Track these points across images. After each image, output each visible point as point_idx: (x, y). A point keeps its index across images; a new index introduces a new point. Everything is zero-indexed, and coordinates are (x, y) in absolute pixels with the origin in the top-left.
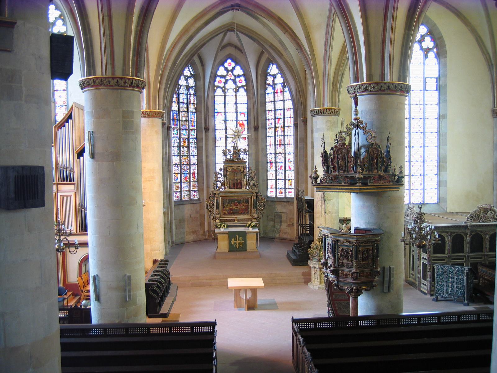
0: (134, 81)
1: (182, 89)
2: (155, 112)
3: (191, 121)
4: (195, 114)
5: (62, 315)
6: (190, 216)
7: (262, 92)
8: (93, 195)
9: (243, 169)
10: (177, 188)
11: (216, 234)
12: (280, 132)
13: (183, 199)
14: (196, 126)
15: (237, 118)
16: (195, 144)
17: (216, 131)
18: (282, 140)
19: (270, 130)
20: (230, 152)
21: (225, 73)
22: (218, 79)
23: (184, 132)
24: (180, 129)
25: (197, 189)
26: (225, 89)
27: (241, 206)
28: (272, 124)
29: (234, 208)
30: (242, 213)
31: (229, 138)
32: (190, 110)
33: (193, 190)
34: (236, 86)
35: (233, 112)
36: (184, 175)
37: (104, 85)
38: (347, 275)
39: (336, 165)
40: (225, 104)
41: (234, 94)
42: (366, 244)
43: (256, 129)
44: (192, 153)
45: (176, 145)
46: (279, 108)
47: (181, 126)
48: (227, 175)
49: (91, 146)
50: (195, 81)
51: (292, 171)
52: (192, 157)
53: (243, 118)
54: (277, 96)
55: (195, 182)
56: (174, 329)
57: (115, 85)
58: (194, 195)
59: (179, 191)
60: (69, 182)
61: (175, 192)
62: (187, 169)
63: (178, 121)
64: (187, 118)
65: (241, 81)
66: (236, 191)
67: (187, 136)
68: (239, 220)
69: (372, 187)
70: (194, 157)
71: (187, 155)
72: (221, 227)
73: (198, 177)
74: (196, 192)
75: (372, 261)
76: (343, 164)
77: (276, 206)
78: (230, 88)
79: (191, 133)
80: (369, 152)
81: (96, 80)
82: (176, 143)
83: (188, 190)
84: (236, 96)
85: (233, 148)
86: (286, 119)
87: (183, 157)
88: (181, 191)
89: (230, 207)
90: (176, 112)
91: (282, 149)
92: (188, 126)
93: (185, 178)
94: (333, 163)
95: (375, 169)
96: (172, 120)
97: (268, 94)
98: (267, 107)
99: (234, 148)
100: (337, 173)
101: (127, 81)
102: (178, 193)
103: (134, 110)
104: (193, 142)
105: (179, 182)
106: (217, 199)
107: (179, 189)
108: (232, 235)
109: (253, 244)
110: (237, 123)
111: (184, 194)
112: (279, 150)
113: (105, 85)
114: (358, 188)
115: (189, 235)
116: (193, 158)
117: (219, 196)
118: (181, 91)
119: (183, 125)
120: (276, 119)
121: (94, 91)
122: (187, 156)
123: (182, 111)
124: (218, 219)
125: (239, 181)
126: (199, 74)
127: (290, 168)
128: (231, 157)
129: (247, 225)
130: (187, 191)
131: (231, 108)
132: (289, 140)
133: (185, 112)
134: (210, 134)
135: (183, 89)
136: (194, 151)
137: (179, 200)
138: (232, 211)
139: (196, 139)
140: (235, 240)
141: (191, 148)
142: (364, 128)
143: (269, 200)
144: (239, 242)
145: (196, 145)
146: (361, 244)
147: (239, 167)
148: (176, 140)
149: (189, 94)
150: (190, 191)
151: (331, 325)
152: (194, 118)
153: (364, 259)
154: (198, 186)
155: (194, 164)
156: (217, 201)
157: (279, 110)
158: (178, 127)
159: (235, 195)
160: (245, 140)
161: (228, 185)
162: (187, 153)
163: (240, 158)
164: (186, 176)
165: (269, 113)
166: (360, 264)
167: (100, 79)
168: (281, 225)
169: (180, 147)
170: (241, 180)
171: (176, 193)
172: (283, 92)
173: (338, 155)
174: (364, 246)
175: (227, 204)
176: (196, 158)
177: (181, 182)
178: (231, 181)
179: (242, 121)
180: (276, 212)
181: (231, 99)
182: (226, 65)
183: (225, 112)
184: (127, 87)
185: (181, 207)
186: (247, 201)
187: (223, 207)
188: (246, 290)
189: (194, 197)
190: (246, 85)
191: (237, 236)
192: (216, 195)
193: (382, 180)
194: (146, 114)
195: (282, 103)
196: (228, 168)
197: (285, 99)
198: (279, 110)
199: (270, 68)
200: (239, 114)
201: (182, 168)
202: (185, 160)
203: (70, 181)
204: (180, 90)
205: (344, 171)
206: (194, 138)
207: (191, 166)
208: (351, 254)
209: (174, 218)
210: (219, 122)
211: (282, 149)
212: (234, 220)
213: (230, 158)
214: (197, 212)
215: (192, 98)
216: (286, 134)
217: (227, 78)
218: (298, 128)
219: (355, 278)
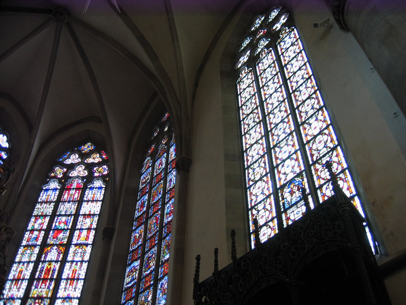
12: (53, 255)
18: (54, 270)
28: (37, 239)
54: (66, 194)
86: (77, 233)
91: (49, 288)
98: (36, 210)
112: (40, 290)
120: (51, 232)
132: (74, 272)
172: (83, 190)
198: (65, 215)
211: (49, 288)
216: (70, 258)
218: (111, 239)
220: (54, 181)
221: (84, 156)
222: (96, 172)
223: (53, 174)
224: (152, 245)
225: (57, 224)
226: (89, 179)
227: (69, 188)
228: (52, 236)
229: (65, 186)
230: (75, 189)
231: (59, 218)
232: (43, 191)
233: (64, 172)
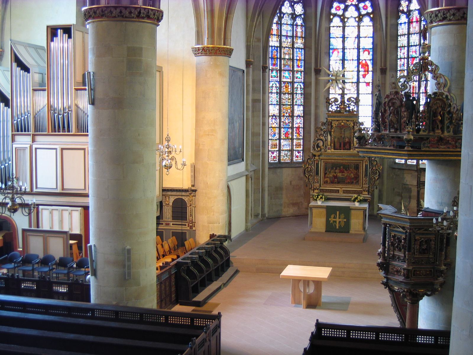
0: (142, 11)
1: (285, 18)
2: (219, 48)
3: (297, 60)
4: (303, 51)
5: (64, 289)
6: (291, 184)
7: (393, 21)
8: (92, 149)
9: (353, 125)
10: (275, 146)
11: (311, 208)
13: (282, 161)
16: (302, 89)
18: (416, 87)
19: (401, 73)
20: (337, 102)
23: (286, 74)
24: (280, 70)
25: (302, 149)
26: (345, 17)
27: (348, 173)
29: (340, 175)
30: (349, 183)
31: (347, 83)
32: (296, 46)
33: (296, 149)
34: (360, 14)
36: (284, 130)
37: (106, 16)
38: (398, 272)
39: (387, 121)
40: (344, 37)
41: (356, 24)
42: (424, 232)
43: (383, 71)
44: (296, 102)
45: (274, 90)
46: (414, 43)
48: (331, 132)
49: (91, 89)
50: (304, 7)
52: (296, 107)
53: (366, 57)
54: (412, 27)
55: (300, 139)
56: (170, 318)
57: (118, 16)
58: (297, 157)
59: (277, 151)
60: (20, 133)
61: (271, 151)
62: (289, 123)
63: (279, 60)
64: (291, 56)
66: (341, 153)
67: (291, 79)
68: (345, 192)
69: (427, 153)
71: (289, 103)
72: (318, 199)
74: (300, 152)
75: (434, 256)
76: (394, 120)
77: (405, 175)
78: (352, 17)
79: (297, 76)
80: (430, 105)
81: (96, 11)
82: (274, 88)
83: (289, 149)
84: (359, 27)
85: (340, 96)
87: (284, 106)
88: (279, 151)
89: (334, 174)
90: (276, 48)
92: (291, 67)
93: (286, 134)
94: (450, 119)
95: (438, 128)
96: (271, 58)
97: (401, 24)
98: (399, 42)
99: (341, 96)
100: (387, 132)
101: (133, 11)
102: (275, 153)
103: (144, 46)
104: (299, 87)
105: (277, 139)
106: (317, 162)
107: (276, 148)
108: (330, 211)
109: (359, 224)
110: (359, 63)
111: (283, 155)
113: (107, 16)
114: (406, 153)
115: (288, 207)
116: (298, 108)
117: (319, 159)
118: (283, 21)
119: (285, 65)
120: (410, 59)
121: (95, 23)
122: (290, 105)
123: (284, 47)
124: (317, 189)
125: (347, 140)
128: (337, 108)
129: (352, 199)
130: (287, 150)
131: (351, 43)
133: (288, 47)
135: (287, 18)
136: (299, 99)
137: (276, 161)
138: (336, 180)
140: (334, 218)
141: (295, 95)
142: (432, 71)
143: (396, 167)
144: (340, 220)
145: (303, 92)
146: (418, 231)
147: (348, 121)
148: (274, 84)
149: (295, 24)
150: (292, 151)
151: (401, 338)
152: (302, 56)
153: (423, 252)
154: (303, 145)
155: (299, 116)
156: (317, 164)
157: (414, 46)
158: (278, 67)
159: (329, 158)
160: (369, 85)
161: (332, 145)
162: (289, 101)
163: (349, 109)
164: (287, 132)
165: (401, 50)
166: (416, 258)
167: (101, 9)
168: (410, 202)
169: (280, 93)
170: (350, 139)
171: (273, 153)
173: (390, 107)
174: (423, 234)
175: (330, 170)
176: (301, 108)
177: (280, 139)
178: (336, 140)
179: (365, 60)
180: (404, 184)
181: (351, 32)
183: (344, 49)
184: (133, 17)
185: (279, 170)
186: (357, 167)
187: (325, 174)
188: (306, 282)
189: (297, 159)
190: (372, 13)
191: (338, 212)
192: (315, 158)
193: (442, 144)
194: (208, 51)
195: (418, 36)
198: (414, 46)
201: (282, 120)
202: (286, 110)
203: (67, 132)
204: (283, 19)
205: (396, 130)
206: (301, 83)
207: (295, 119)
208: (404, 243)
209: (266, 185)
210: (335, 62)
212: (338, 191)
213: (336, 109)
215: (299, 29)
217: (347, 4)
219: (407, 276)
230: (416, 21)
231: (412, 48)
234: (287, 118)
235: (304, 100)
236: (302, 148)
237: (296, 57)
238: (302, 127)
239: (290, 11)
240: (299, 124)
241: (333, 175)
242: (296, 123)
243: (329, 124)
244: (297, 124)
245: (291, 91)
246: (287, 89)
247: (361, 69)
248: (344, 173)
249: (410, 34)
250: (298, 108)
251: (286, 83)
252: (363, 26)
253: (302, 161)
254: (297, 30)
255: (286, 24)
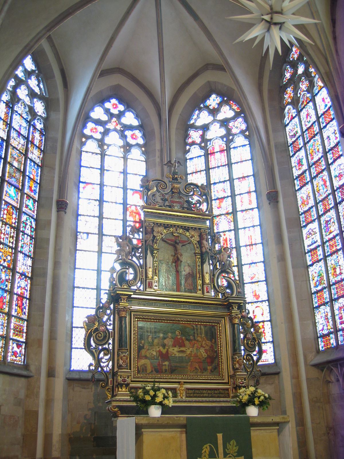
4: (40, 170)
7: (180, 155)
14: (38, 194)
15: (125, 199)
16: (32, 229)
17: (79, 217)
21: (104, 118)
22: (90, 125)
27: (193, 347)
29: (175, 351)
31: (106, 235)
32: (30, 155)
35: (118, 187)
47: (7, 175)
50: (47, 109)
51: (262, 301)
52: (20, 256)
58: (15, 354)
62: (7, 280)
64: (22, 168)
65: (136, 136)
67: (17, 202)
70: (26, 258)
71: (11, 245)
73: (29, 309)
74: (21, 346)
79: (27, 203)
84: (125, 158)
86: (238, 198)
89: (161, 348)
92: (21, 184)
110: (125, 210)
116: (24, 260)
119: (11, 176)
122: (12, 248)
126: (58, 100)
127: (257, 296)
132: (250, 238)
133: (20, 152)
134: (68, 217)
135: (23, 108)
138: (167, 363)
139: (36, 220)
145: (33, 234)
147: (187, 229)
149: (32, 123)
154: (26, 333)
157: (220, 182)
162: (12, 241)
175: (150, 339)
176: (29, 262)
179: (136, 206)
182: (108, 105)
183: (102, 185)
187: (140, 348)
189: (15, 358)
190: (145, 145)
191: (220, 436)
196: (156, 229)
197: (233, 161)
198: (220, 182)
199: (195, 117)
200: (129, 192)
206: (32, 218)
214: (19, 403)
215: (37, 135)
217: (107, 127)
218: (277, 202)
220: (195, 148)
221: (214, 112)
222: (232, 128)
223: (190, 141)
224: (326, 209)
225: (216, 193)
226: (228, 137)
227: (212, 152)
228: (215, 206)
229: (208, 151)
230: (219, 151)
232: (188, 161)
233: (201, 135)
234: (3, 270)
235: (35, 248)
236: (24, 338)
237: (29, 172)
238: (28, 297)
239: (27, 100)
240: (24, 290)
241: (160, 351)
242: (19, 285)
243: (149, 230)
244: (19, 289)
245: (16, 224)
246: (9, 216)
247: (129, 218)
248: (184, 345)
249: (211, 168)
250: (24, 260)
251: (10, 206)
252: (132, 159)
253: (22, 363)
254: (34, 134)
255: (19, 114)
